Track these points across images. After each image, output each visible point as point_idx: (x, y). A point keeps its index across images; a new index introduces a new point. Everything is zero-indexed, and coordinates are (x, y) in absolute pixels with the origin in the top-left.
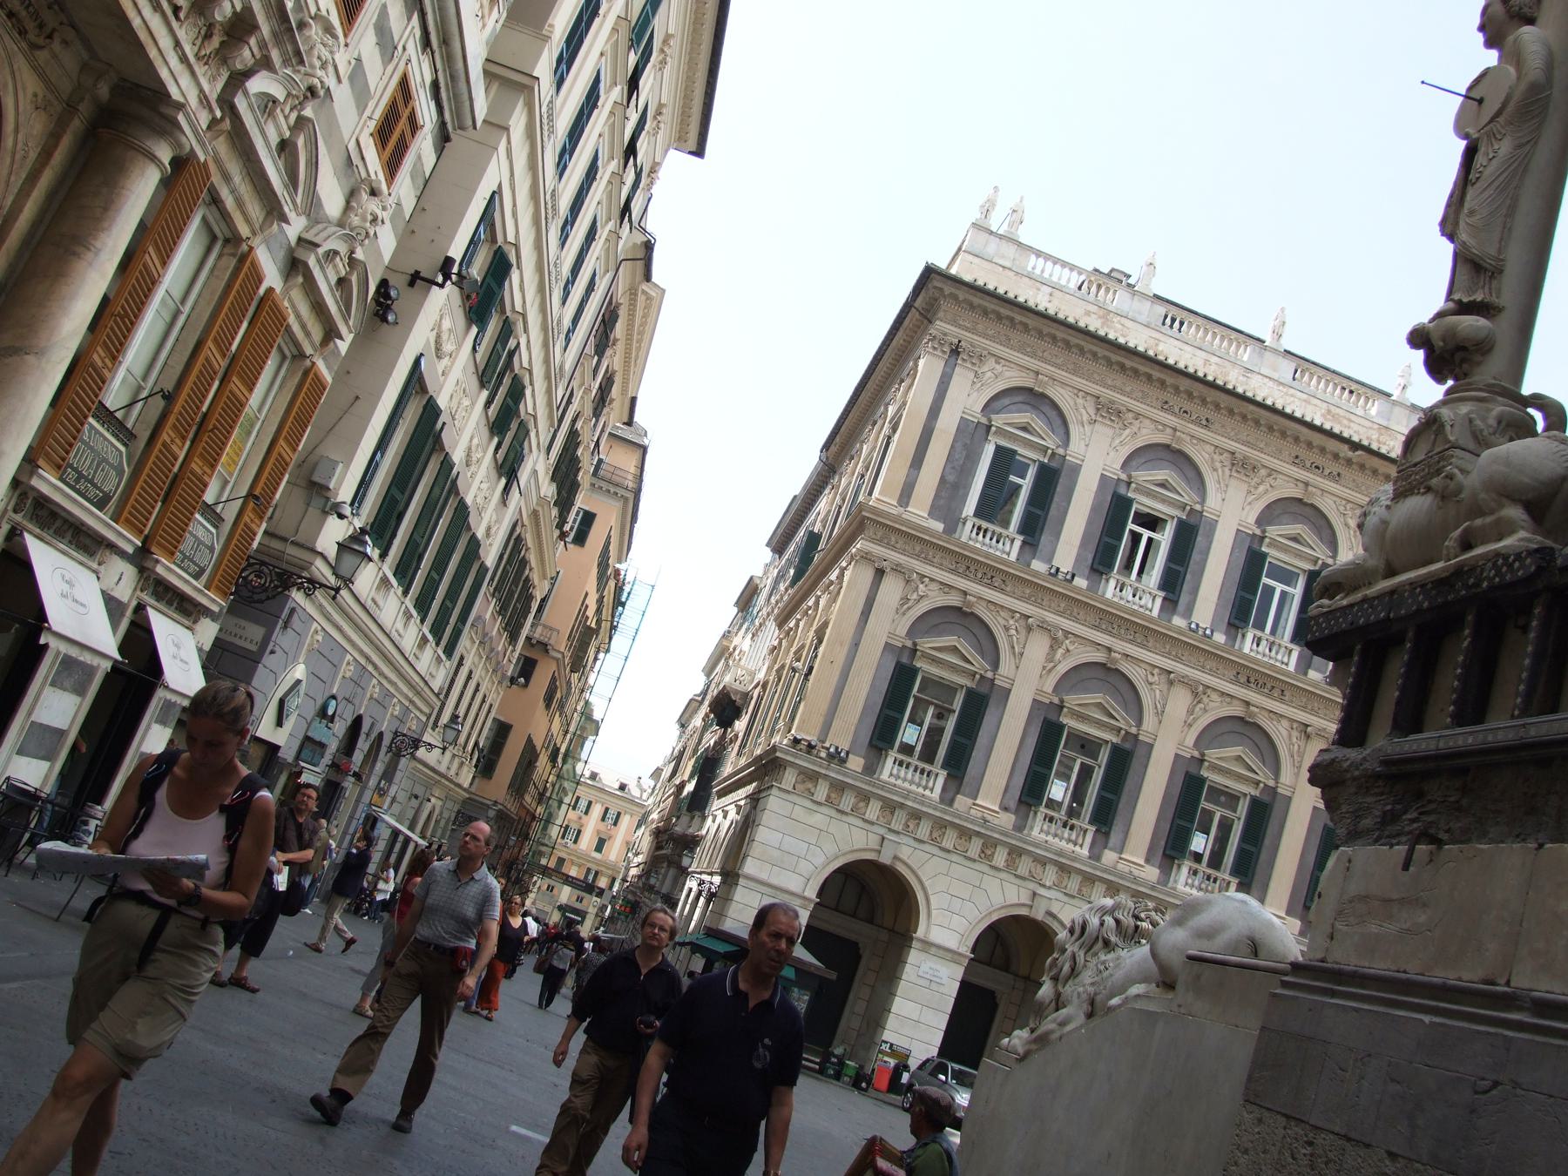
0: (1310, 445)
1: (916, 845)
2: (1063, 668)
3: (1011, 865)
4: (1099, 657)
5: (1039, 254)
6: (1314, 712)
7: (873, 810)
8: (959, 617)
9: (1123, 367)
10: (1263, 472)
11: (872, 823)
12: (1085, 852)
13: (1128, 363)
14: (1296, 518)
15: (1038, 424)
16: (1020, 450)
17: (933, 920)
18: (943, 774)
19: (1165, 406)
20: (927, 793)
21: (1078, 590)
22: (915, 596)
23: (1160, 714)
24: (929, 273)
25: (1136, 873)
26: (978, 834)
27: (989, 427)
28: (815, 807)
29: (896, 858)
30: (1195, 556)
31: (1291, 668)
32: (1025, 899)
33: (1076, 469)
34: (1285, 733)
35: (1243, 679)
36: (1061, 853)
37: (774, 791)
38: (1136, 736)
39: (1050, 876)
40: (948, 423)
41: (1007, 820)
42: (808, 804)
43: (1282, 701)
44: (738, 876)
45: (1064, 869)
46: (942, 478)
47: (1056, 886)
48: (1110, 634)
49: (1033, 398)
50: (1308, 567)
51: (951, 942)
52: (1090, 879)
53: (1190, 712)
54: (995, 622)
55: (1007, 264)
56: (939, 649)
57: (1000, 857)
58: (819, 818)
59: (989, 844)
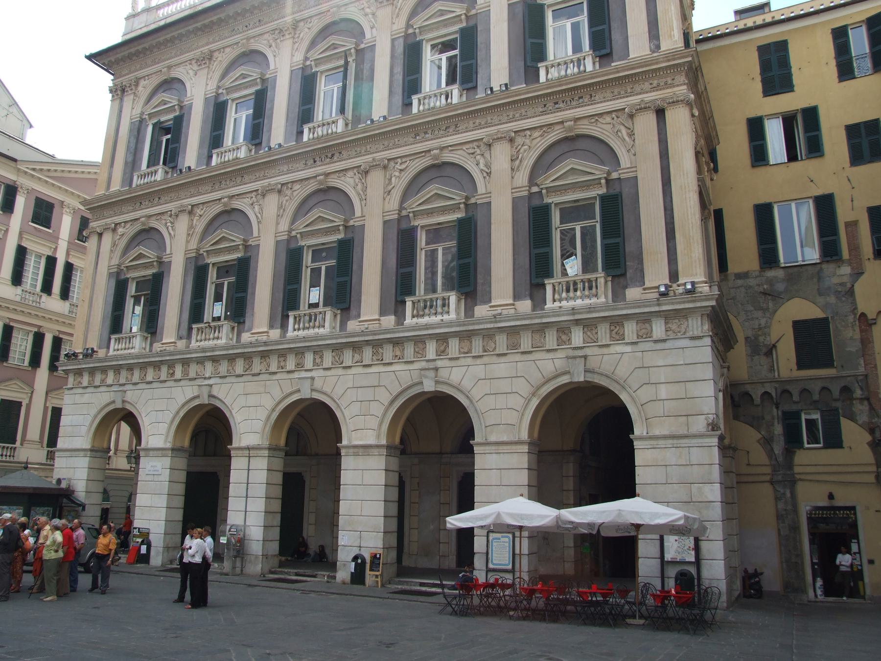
16: (162, 119)
20: (133, 351)
29: (124, 401)
35: (311, 162)
42: (80, 391)
45: (215, 360)
51: (161, 445)
59: (171, 365)
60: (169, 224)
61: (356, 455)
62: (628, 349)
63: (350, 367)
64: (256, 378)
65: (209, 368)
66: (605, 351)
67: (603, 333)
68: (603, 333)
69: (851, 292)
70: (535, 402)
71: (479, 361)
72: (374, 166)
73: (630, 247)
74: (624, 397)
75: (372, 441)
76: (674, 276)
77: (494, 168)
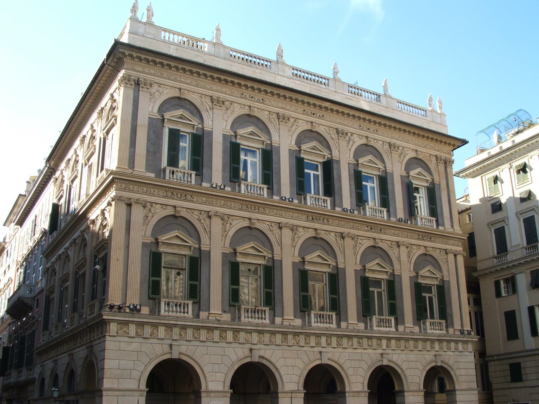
0: (309, 103)
1: (188, 343)
2: (231, 233)
3: (235, 338)
4: (246, 223)
5: (165, 30)
6: (342, 226)
8: (174, 220)
9: (219, 79)
11: (163, 339)
12: (267, 321)
13: (223, 77)
14: (311, 139)
15: (187, 114)
16: (182, 129)
17: (208, 379)
18: (190, 302)
19: (242, 96)
21: (227, 193)
22: (150, 214)
23: (281, 244)
24: (117, 44)
25: (292, 324)
26: (216, 328)
27: (163, 120)
28: (131, 340)
29: (180, 353)
30: (274, 165)
31: (329, 207)
32: (247, 353)
33: (211, 133)
34: (334, 239)
35: (310, 218)
36: (257, 325)
37: (107, 338)
38: (273, 258)
40: (143, 120)
41: (227, 317)
42: (127, 339)
43: (329, 225)
44: (101, 391)
45: (260, 332)
46: (148, 151)
47: (259, 342)
48: (248, 211)
49: (179, 101)
50: (322, 160)
51: (221, 388)
52: (273, 333)
53: (293, 240)
54: (193, 218)
55: (152, 37)
56: (169, 239)
57: (230, 335)
59: (223, 330)
60: (203, 221)
61: (353, 396)
62: (452, 353)
63: (346, 348)
64: (290, 348)
65: (255, 337)
66: (445, 353)
70: (425, 373)
71: (403, 352)
73: (448, 311)
74: (452, 373)
75: (360, 389)
77: (402, 259)
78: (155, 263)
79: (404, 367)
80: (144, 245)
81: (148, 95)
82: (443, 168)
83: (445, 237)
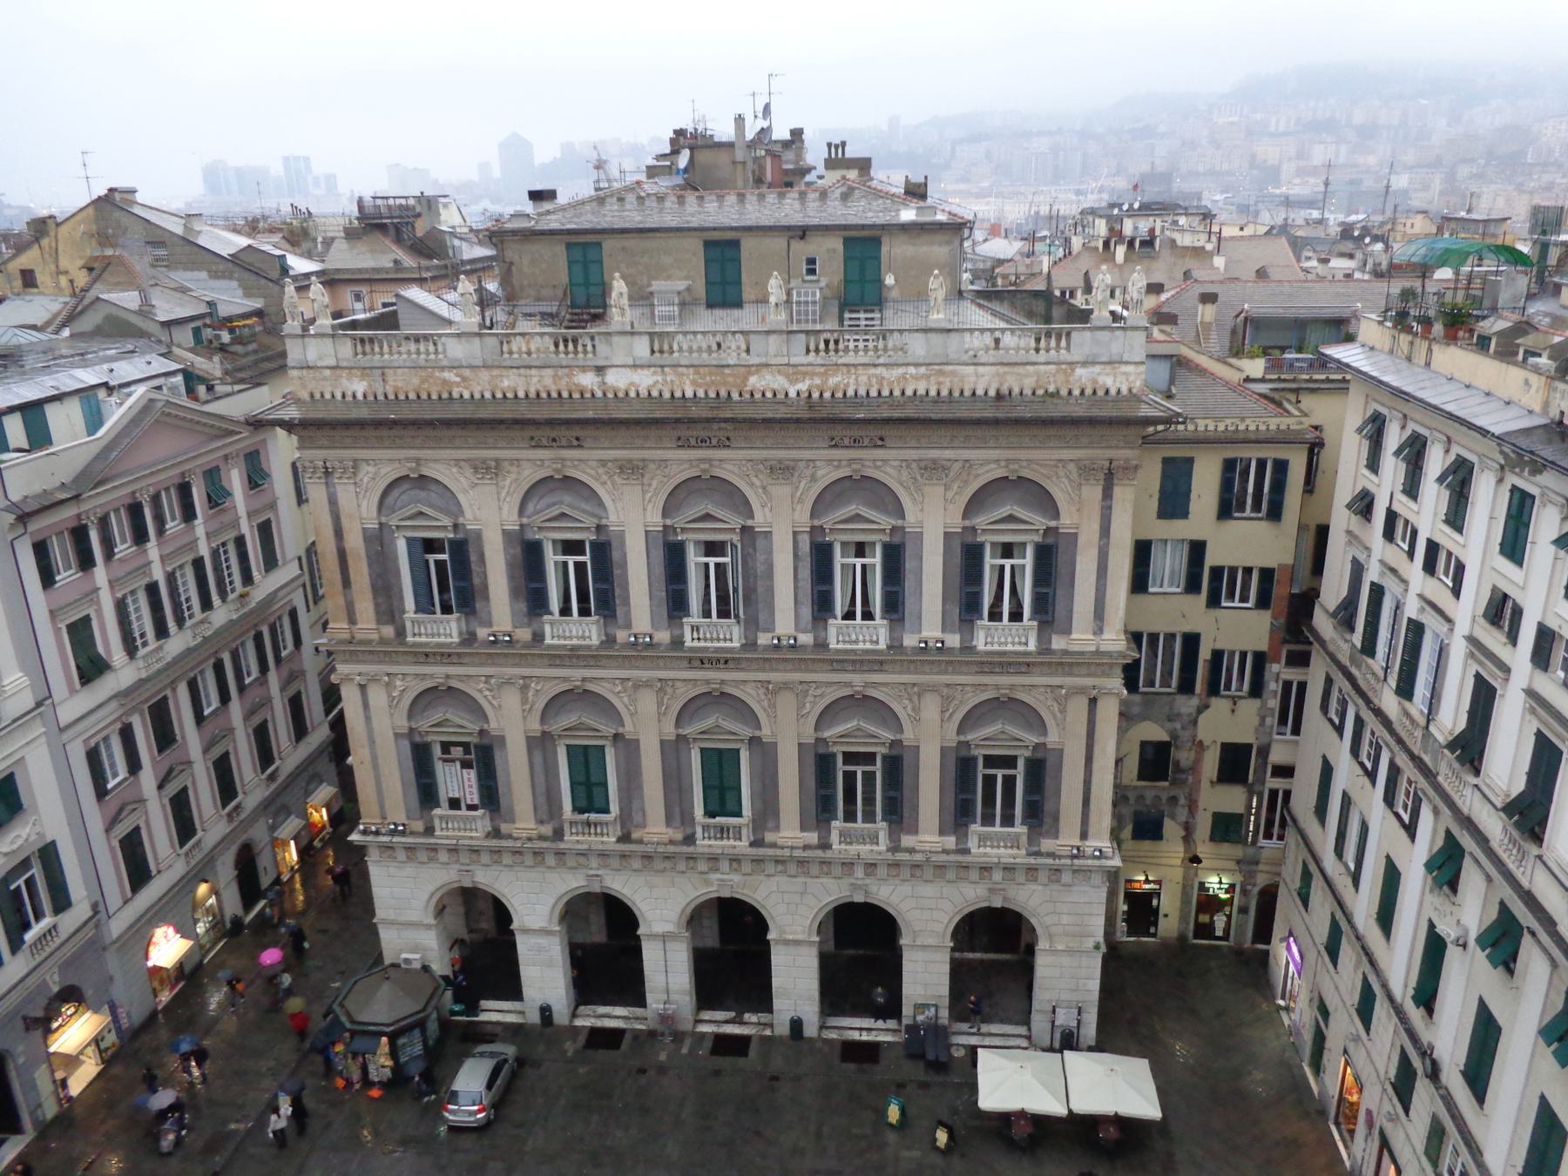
2: (540, 705)
7: (443, 856)
10: (652, 466)
30: (617, 572)
33: (478, 535)
34: (753, 692)
39: (594, 862)
47: (605, 866)
58: (409, 870)
67: (1020, 876)
68: (1020, 876)
69: (1195, 722)
72: (786, 686)
73: (1048, 807)
76: (1084, 836)
78: (422, 759)
79: (904, 907)
80: (397, 736)
81: (352, 488)
82: (1098, 492)
83: (1070, 663)
